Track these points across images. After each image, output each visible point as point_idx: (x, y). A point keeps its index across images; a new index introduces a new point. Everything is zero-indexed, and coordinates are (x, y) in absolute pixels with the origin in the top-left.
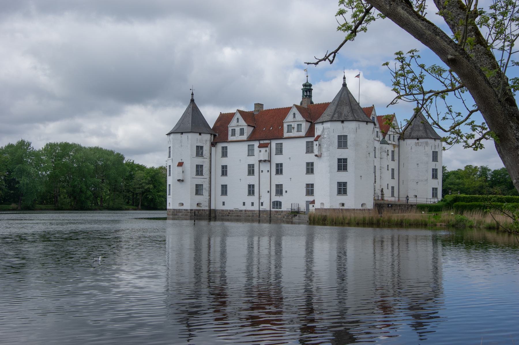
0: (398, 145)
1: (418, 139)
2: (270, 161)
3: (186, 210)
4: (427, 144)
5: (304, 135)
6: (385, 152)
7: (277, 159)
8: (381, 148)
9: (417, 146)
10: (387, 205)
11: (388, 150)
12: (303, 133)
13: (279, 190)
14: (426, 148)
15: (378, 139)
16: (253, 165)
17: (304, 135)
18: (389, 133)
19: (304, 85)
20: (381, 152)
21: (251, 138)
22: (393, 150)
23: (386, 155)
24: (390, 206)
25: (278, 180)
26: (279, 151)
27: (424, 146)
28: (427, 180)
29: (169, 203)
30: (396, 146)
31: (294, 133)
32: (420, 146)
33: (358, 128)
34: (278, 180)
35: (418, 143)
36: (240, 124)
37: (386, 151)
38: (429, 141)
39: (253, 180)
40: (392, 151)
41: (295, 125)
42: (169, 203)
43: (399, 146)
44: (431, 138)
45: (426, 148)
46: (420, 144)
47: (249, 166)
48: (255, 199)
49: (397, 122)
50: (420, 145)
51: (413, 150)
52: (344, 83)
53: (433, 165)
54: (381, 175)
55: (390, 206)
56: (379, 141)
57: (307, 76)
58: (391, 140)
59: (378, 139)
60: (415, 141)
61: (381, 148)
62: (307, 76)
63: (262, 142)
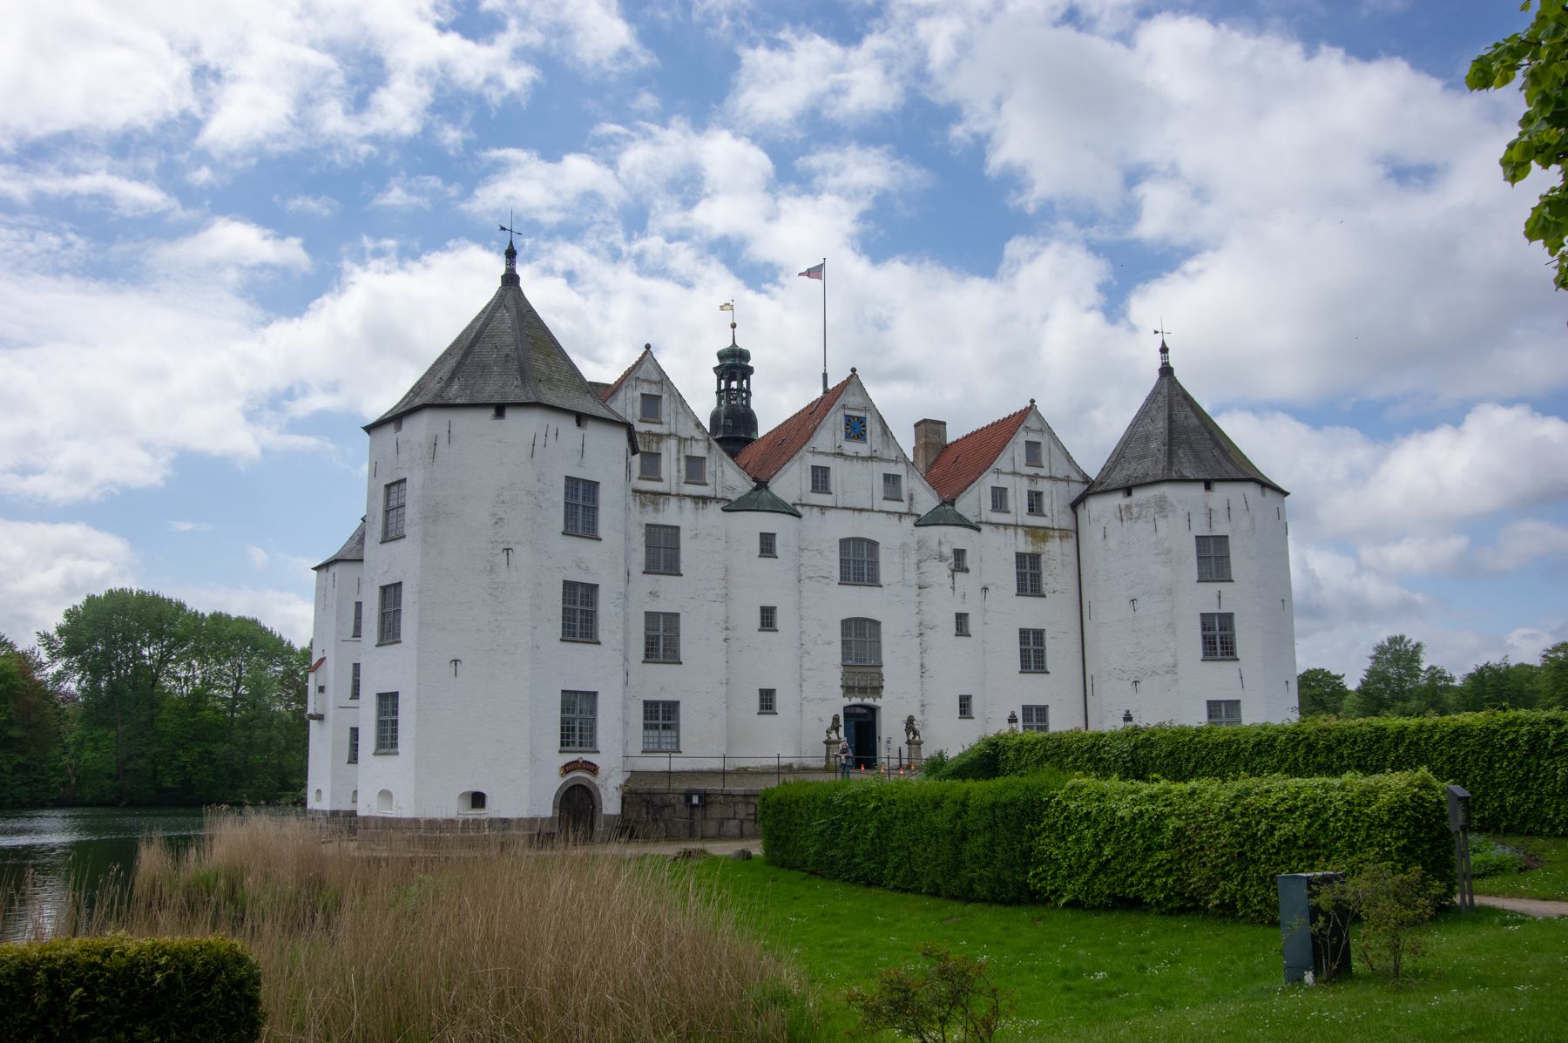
0: (1072, 527)
1: (1128, 491)
3: (324, 812)
4: (1162, 506)
6: (941, 558)
8: (919, 542)
9: (1125, 523)
10: (682, 798)
11: (959, 554)
14: (1161, 523)
15: (902, 507)
18: (989, 480)
19: (721, 356)
20: (920, 561)
22: (1029, 549)
23: (950, 572)
24: (695, 800)
27: (1151, 519)
28: (1175, 666)
29: (319, 791)
30: (1056, 533)
32: (1138, 518)
33: (442, 441)
35: (1128, 507)
37: (947, 551)
38: (1170, 491)
40: (1020, 557)
42: (319, 791)
43: (1074, 533)
44: (1184, 480)
45: (1161, 523)
46: (1135, 510)
49: (1053, 434)
50: (1135, 515)
51: (1112, 543)
52: (507, 270)
53: (1207, 598)
54: (927, 664)
55: (695, 800)
56: (909, 514)
57: (734, 326)
58: (1011, 506)
59: (902, 507)
60: (1119, 499)
61: (921, 544)
62: (734, 326)
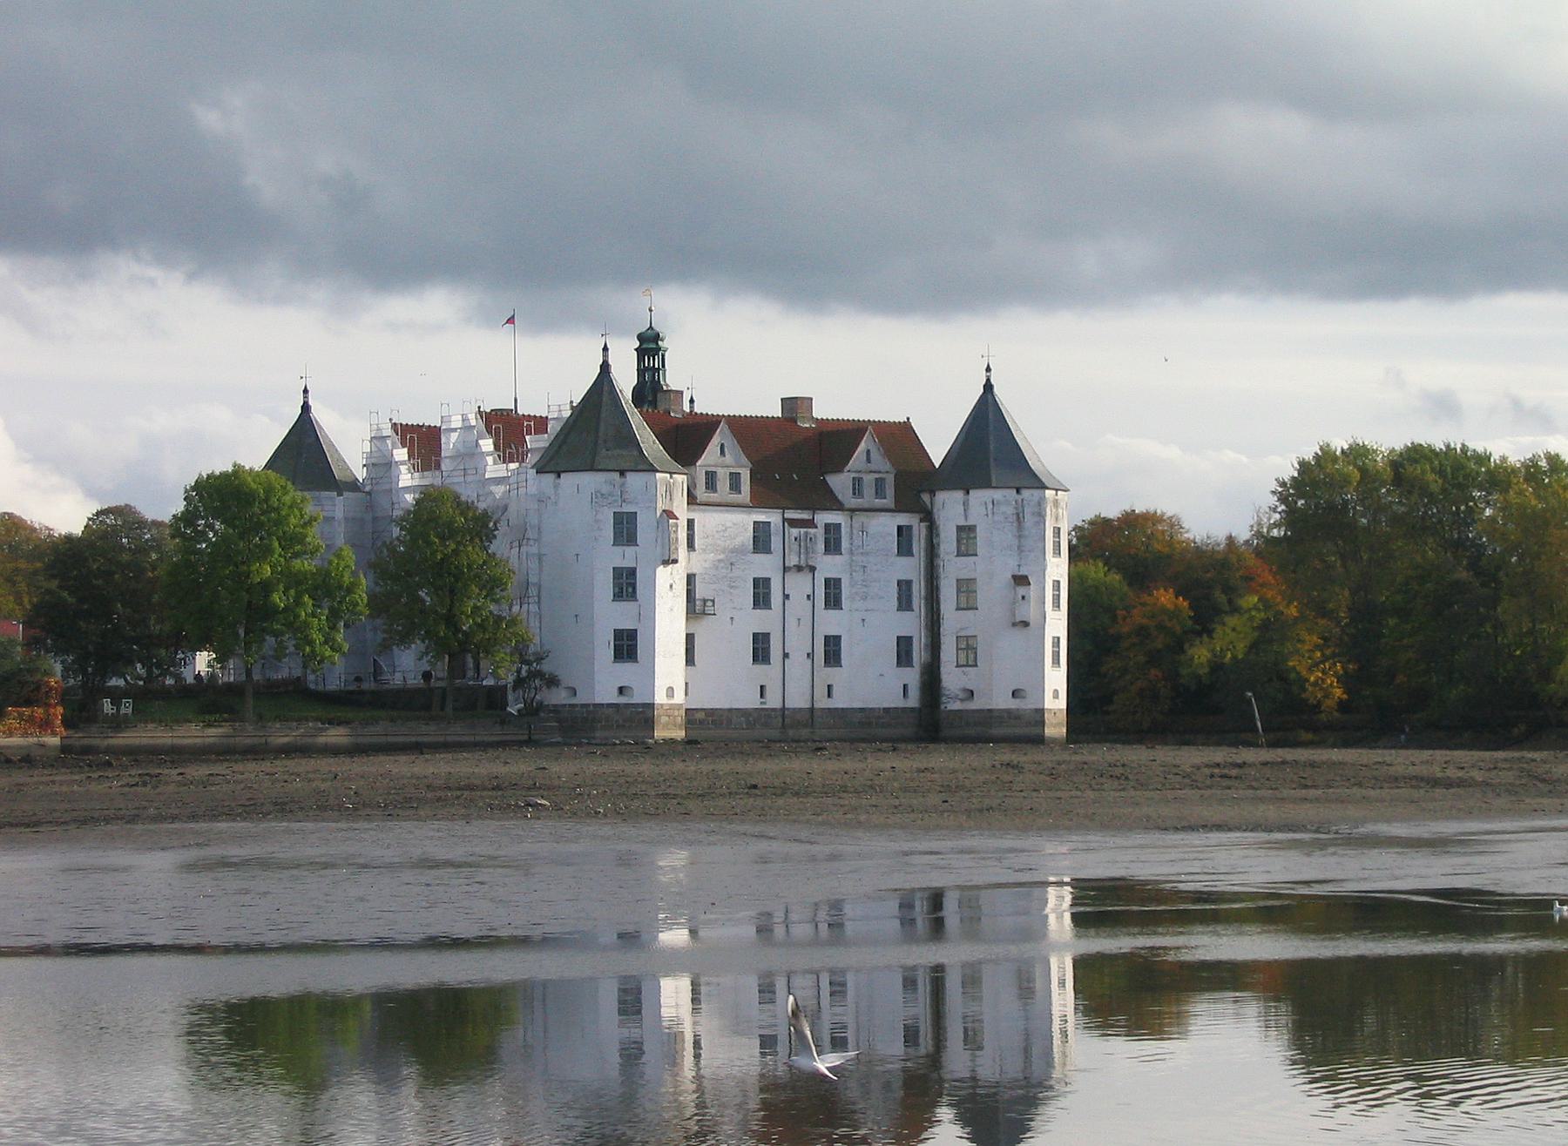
2: (813, 569)
5: (892, 506)
7: (829, 566)
12: (889, 501)
13: (833, 651)
16: (767, 581)
17: (892, 506)
21: (758, 502)
25: (831, 622)
26: (833, 544)
31: (869, 498)
34: (831, 622)
36: (729, 459)
39: (765, 621)
41: (869, 479)
47: (757, 582)
48: (769, 674)
63: (790, 514)
